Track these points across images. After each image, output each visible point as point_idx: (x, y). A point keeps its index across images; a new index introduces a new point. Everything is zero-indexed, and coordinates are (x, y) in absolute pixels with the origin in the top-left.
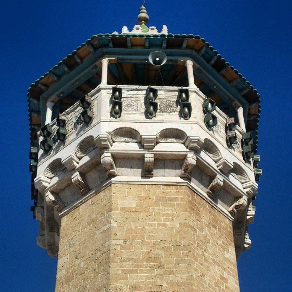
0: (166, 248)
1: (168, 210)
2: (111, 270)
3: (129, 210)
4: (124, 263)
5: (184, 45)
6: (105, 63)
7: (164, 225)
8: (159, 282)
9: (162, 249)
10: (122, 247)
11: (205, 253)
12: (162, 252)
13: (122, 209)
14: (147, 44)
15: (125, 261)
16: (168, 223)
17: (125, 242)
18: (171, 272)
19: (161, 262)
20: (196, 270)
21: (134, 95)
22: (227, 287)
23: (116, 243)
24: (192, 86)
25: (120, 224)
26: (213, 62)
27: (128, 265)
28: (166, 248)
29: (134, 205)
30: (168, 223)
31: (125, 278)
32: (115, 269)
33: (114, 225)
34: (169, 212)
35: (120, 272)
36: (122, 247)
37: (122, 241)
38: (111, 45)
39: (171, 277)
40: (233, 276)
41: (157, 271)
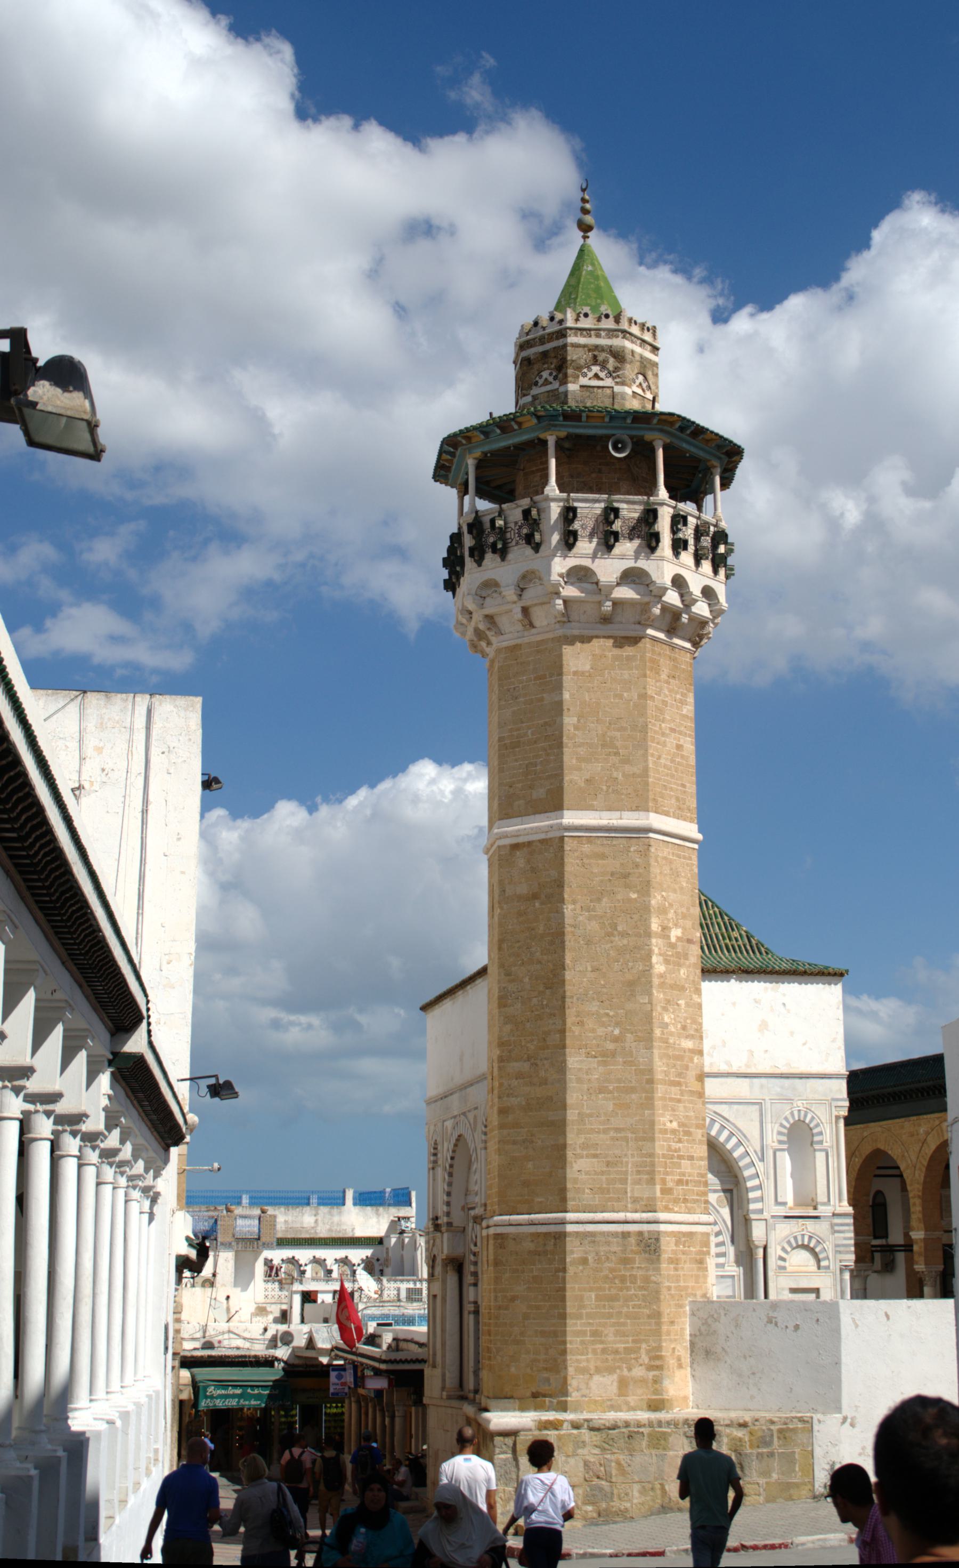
0: (623, 729)
1: (626, 674)
2: (566, 758)
3: (583, 673)
4: (579, 749)
5: (655, 421)
6: (551, 441)
7: (621, 697)
8: (615, 774)
9: (618, 730)
10: (576, 728)
11: (663, 725)
12: (618, 734)
13: (575, 673)
14: (607, 419)
15: (579, 746)
16: (625, 694)
17: (579, 721)
18: (626, 761)
19: (617, 748)
20: (652, 755)
21: (590, 508)
22: (682, 757)
23: (569, 721)
24: (663, 493)
25: (572, 695)
26: (688, 432)
27: (582, 751)
28: (623, 729)
29: (588, 667)
30: (625, 694)
31: (579, 769)
32: (569, 758)
33: (566, 696)
34: (626, 677)
35: (574, 761)
36: (576, 728)
37: (576, 719)
38: (561, 418)
39: (627, 768)
40: (690, 736)
41: (614, 759)
